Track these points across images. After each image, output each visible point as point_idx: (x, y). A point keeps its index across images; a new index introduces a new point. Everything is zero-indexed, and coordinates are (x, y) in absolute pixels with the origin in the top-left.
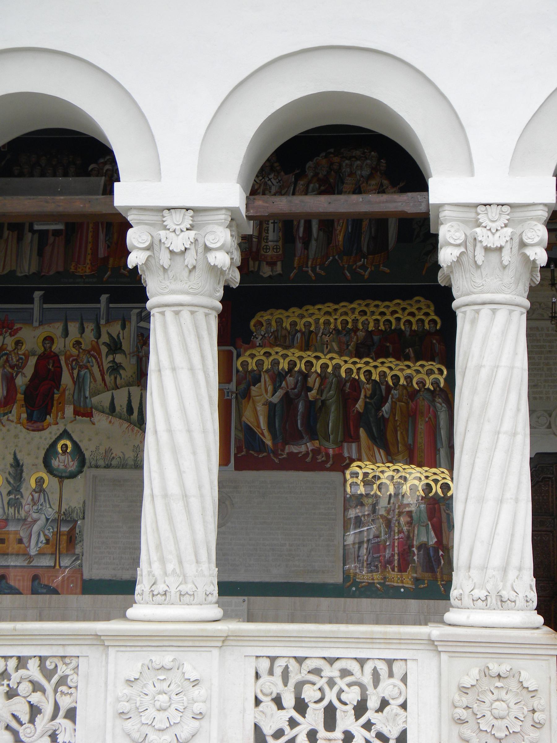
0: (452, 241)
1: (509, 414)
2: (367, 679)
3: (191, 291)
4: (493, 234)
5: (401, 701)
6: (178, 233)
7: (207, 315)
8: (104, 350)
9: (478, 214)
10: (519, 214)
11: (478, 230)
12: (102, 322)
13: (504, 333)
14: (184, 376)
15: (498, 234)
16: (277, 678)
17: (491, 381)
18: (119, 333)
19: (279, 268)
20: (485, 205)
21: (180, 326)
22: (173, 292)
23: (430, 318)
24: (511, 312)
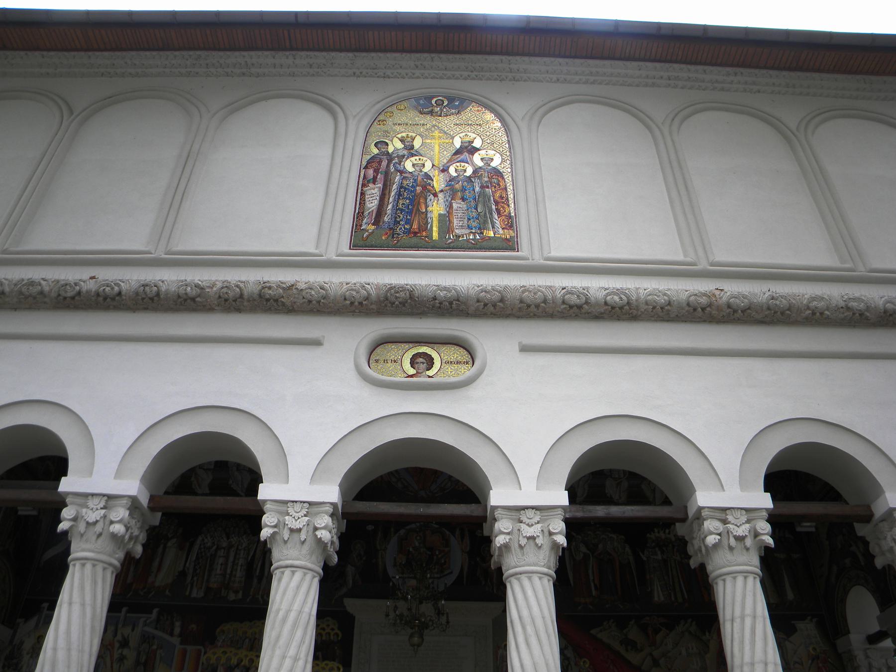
0: (269, 524)
1: (295, 644)
3: (96, 550)
4: (296, 520)
6: (94, 510)
7: (104, 569)
8: (117, 645)
9: (288, 507)
10: (315, 509)
11: (287, 518)
12: (120, 626)
13: (298, 587)
14: (76, 608)
15: (299, 521)
17: (284, 620)
18: (129, 635)
19: (240, 595)
20: (293, 502)
21: (82, 573)
22: (83, 550)
23: (334, 632)
24: (305, 574)
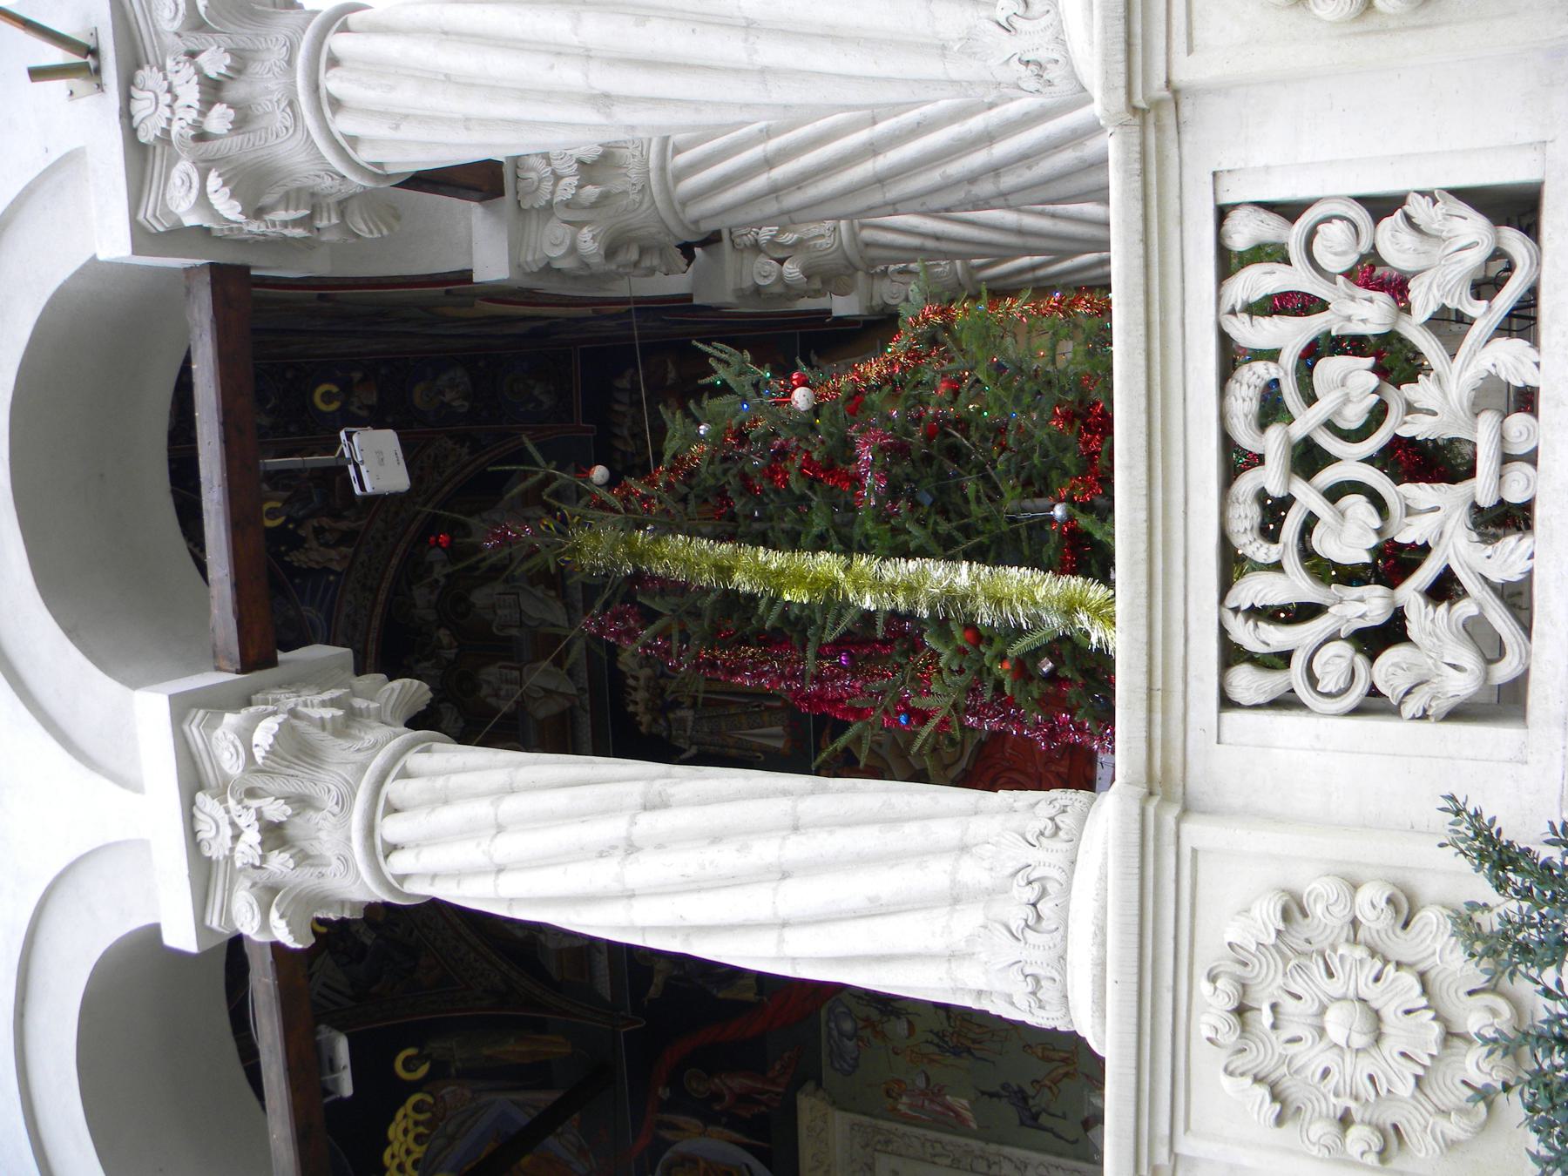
2: (1290, 334)
5: (1361, 215)
14: (508, 847)
16: (1299, 637)
